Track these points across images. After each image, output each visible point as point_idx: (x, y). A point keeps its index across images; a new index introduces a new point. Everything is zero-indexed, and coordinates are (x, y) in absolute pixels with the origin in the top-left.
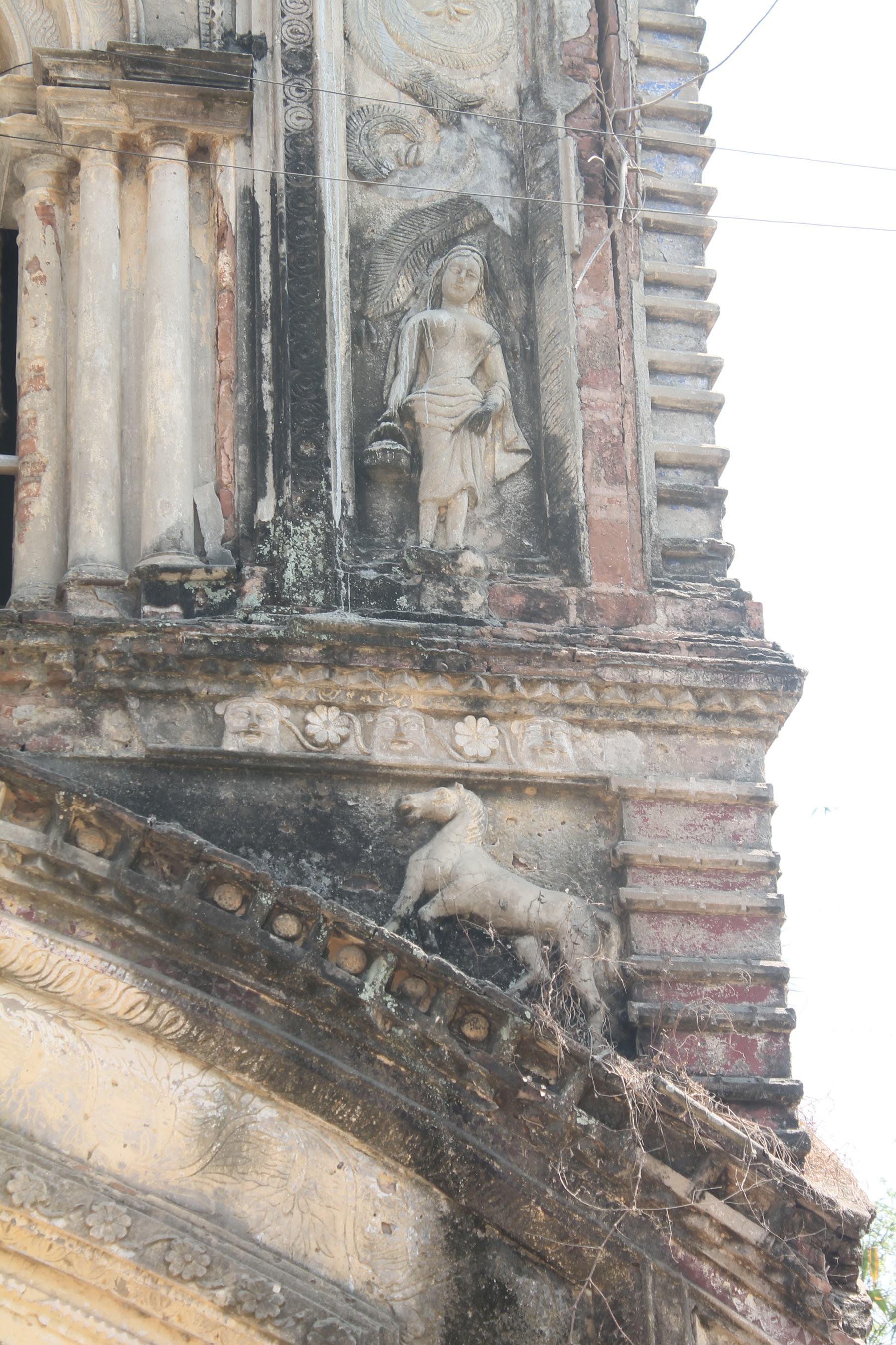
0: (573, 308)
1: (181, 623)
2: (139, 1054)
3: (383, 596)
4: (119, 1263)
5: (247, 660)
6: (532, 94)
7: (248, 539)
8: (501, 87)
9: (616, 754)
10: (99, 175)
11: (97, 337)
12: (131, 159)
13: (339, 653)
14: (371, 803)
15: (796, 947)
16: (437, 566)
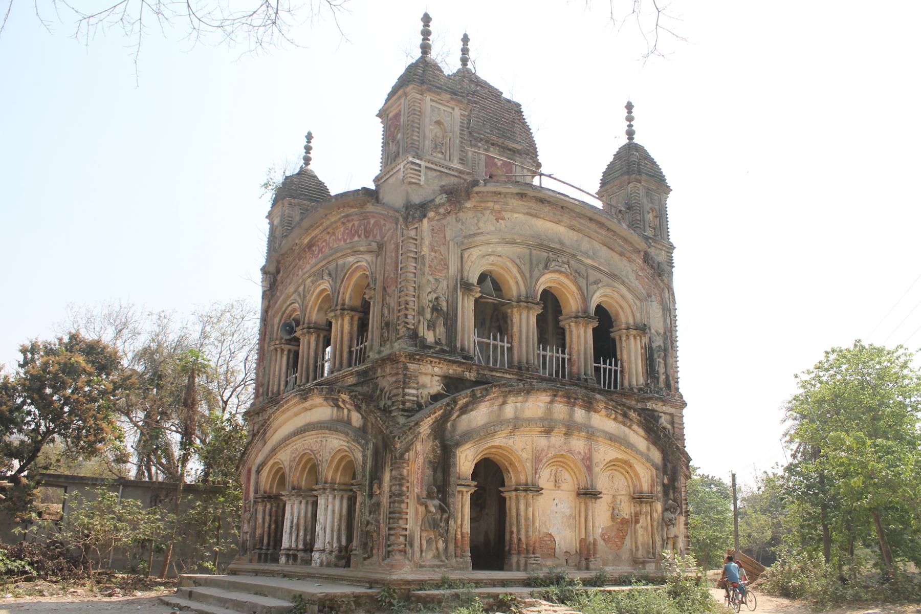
0: (670, 360)
1: (643, 394)
2: (641, 439)
3: (657, 392)
4: (644, 460)
5: (650, 399)
6: (665, 333)
7: (647, 384)
8: (662, 331)
9: (672, 410)
10: (632, 338)
11: (633, 358)
12: (635, 338)
13: (657, 399)
14: (656, 414)
15: (685, 432)
16: (661, 389)
